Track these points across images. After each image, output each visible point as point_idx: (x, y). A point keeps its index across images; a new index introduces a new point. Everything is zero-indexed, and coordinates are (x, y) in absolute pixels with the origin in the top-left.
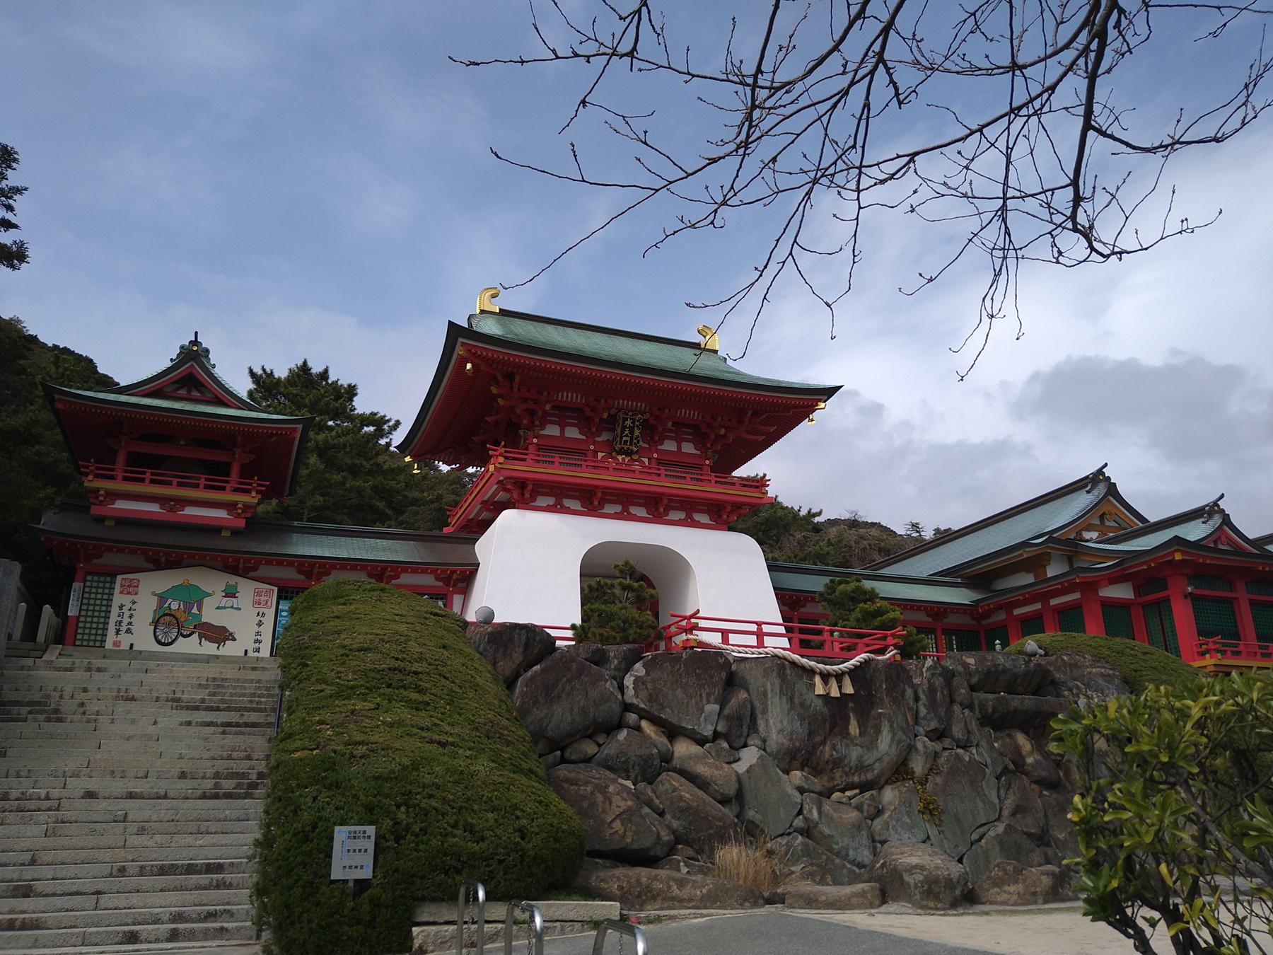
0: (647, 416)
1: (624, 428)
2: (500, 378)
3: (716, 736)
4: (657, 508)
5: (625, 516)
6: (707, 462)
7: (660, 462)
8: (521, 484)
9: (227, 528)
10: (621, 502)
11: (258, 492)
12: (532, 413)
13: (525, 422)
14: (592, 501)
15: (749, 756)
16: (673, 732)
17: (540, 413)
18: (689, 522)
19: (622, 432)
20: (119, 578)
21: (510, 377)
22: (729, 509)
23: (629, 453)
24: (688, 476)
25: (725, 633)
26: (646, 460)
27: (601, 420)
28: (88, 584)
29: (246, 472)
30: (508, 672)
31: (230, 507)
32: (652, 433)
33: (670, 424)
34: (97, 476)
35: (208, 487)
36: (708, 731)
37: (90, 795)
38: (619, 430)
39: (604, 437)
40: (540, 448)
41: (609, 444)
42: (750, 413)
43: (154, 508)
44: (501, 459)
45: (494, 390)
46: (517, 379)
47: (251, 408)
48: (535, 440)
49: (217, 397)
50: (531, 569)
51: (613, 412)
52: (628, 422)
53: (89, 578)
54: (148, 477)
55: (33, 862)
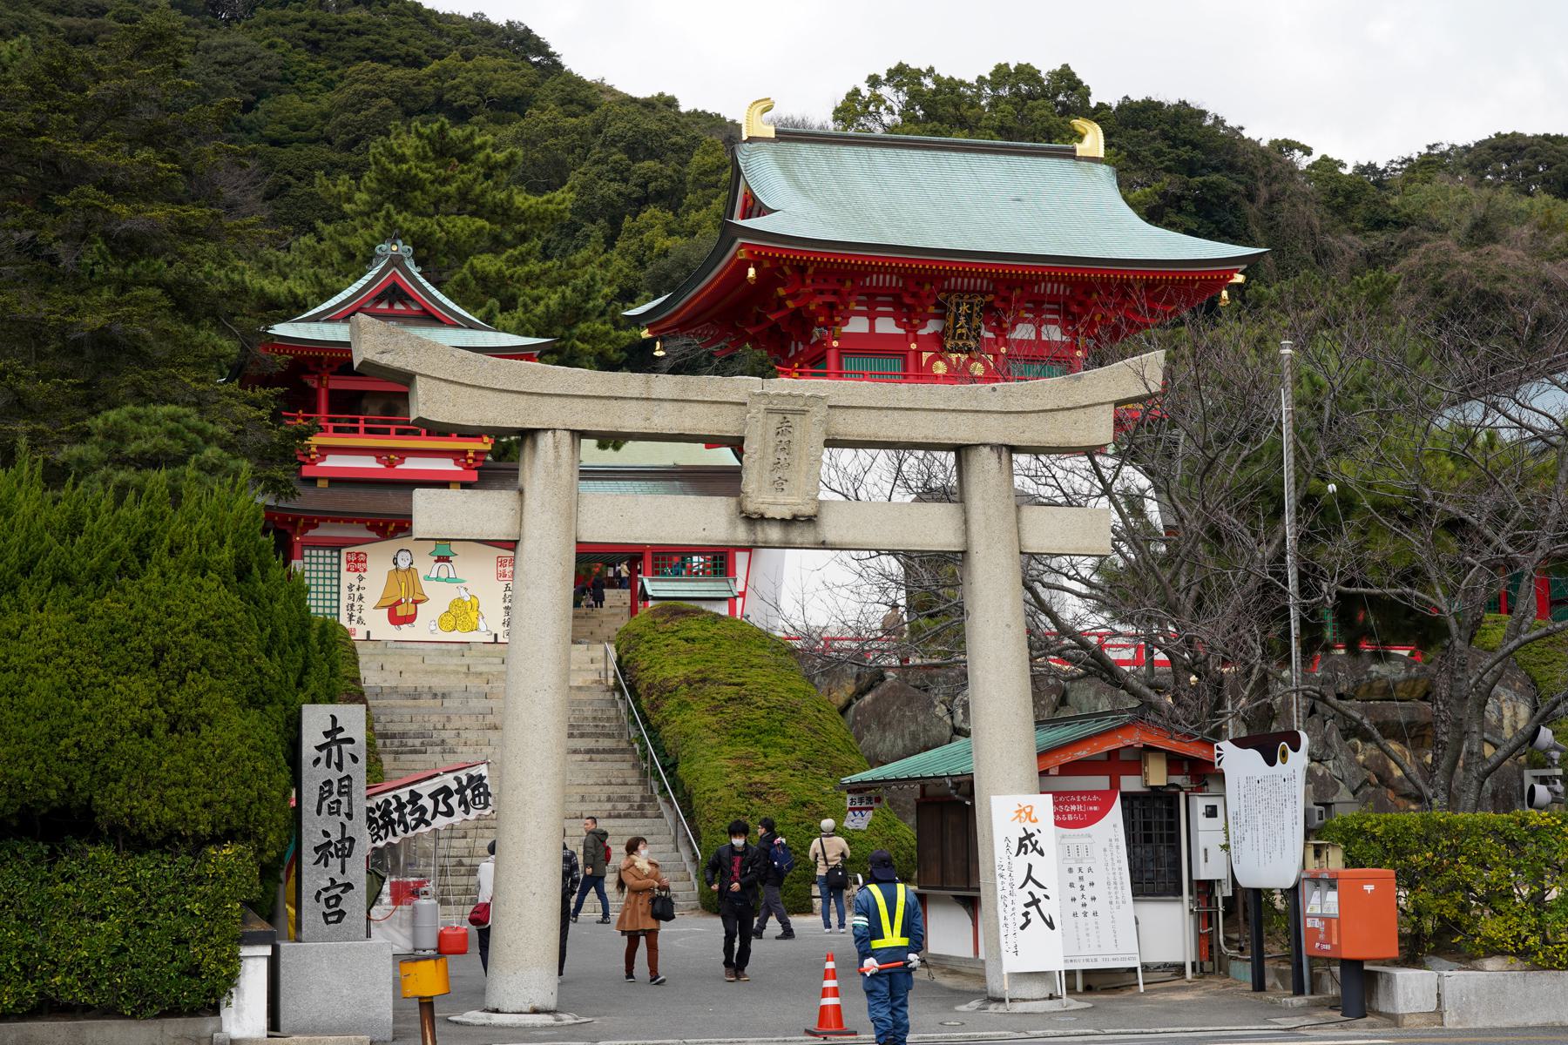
0: (990, 298)
19: (957, 320)
20: (344, 551)
28: (307, 560)
30: (842, 702)
38: (951, 319)
39: (932, 327)
43: (369, 463)
48: (835, 344)
52: (964, 308)
53: (307, 552)
54: (361, 425)
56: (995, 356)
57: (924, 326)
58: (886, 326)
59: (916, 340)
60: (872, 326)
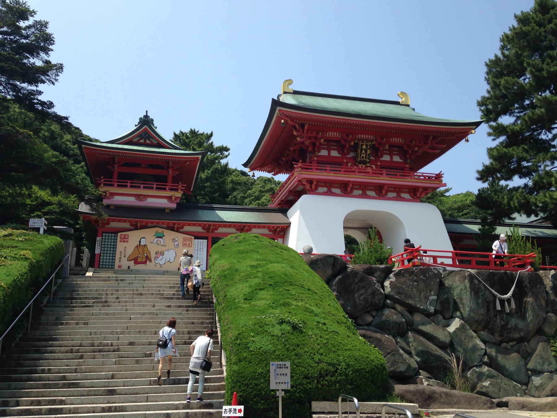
0: (374, 143)
1: (362, 150)
2: (297, 126)
3: (436, 312)
4: (381, 192)
5: (364, 196)
6: (407, 166)
7: (382, 167)
8: (310, 181)
9: (168, 208)
10: (363, 190)
11: (182, 190)
12: (314, 144)
13: (310, 149)
14: (346, 189)
15: (455, 324)
16: (412, 310)
17: (318, 144)
18: (399, 198)
19: (361, 152)
20: (119, 234)
21: (302, 126)
22: (421, 190)
23: (364, 163)
24: (398, 174)
25: (435, 258)
26: (374, 166)
27: (350, 146)
28: (104, 237)
29: (176, 180)
31: (169, 198)
32: (376, 151)
33: (387, 146)
34: (105, 185)
35: (157, 189)
36: (432, 309)
37: (131, 344)
38: (359, 151)
39: (351, 155)
40: (318, 162)
41: (355, 159)
42: (431, 138)
43: (132, 199)
44: (299, 169)
45: (295, 133)
46: (306, 127)
47: (176, 148)
48: (316, 159)
49: (158, 143)
50: (316, 226)
51: (356, 141)
52: (364, 147)
53: (104, 234)
55: (113, 377)
56: (376, 166)
57: (349, 154)
58: (334, 153)
59: (346, 158)
60: (329, 153)
